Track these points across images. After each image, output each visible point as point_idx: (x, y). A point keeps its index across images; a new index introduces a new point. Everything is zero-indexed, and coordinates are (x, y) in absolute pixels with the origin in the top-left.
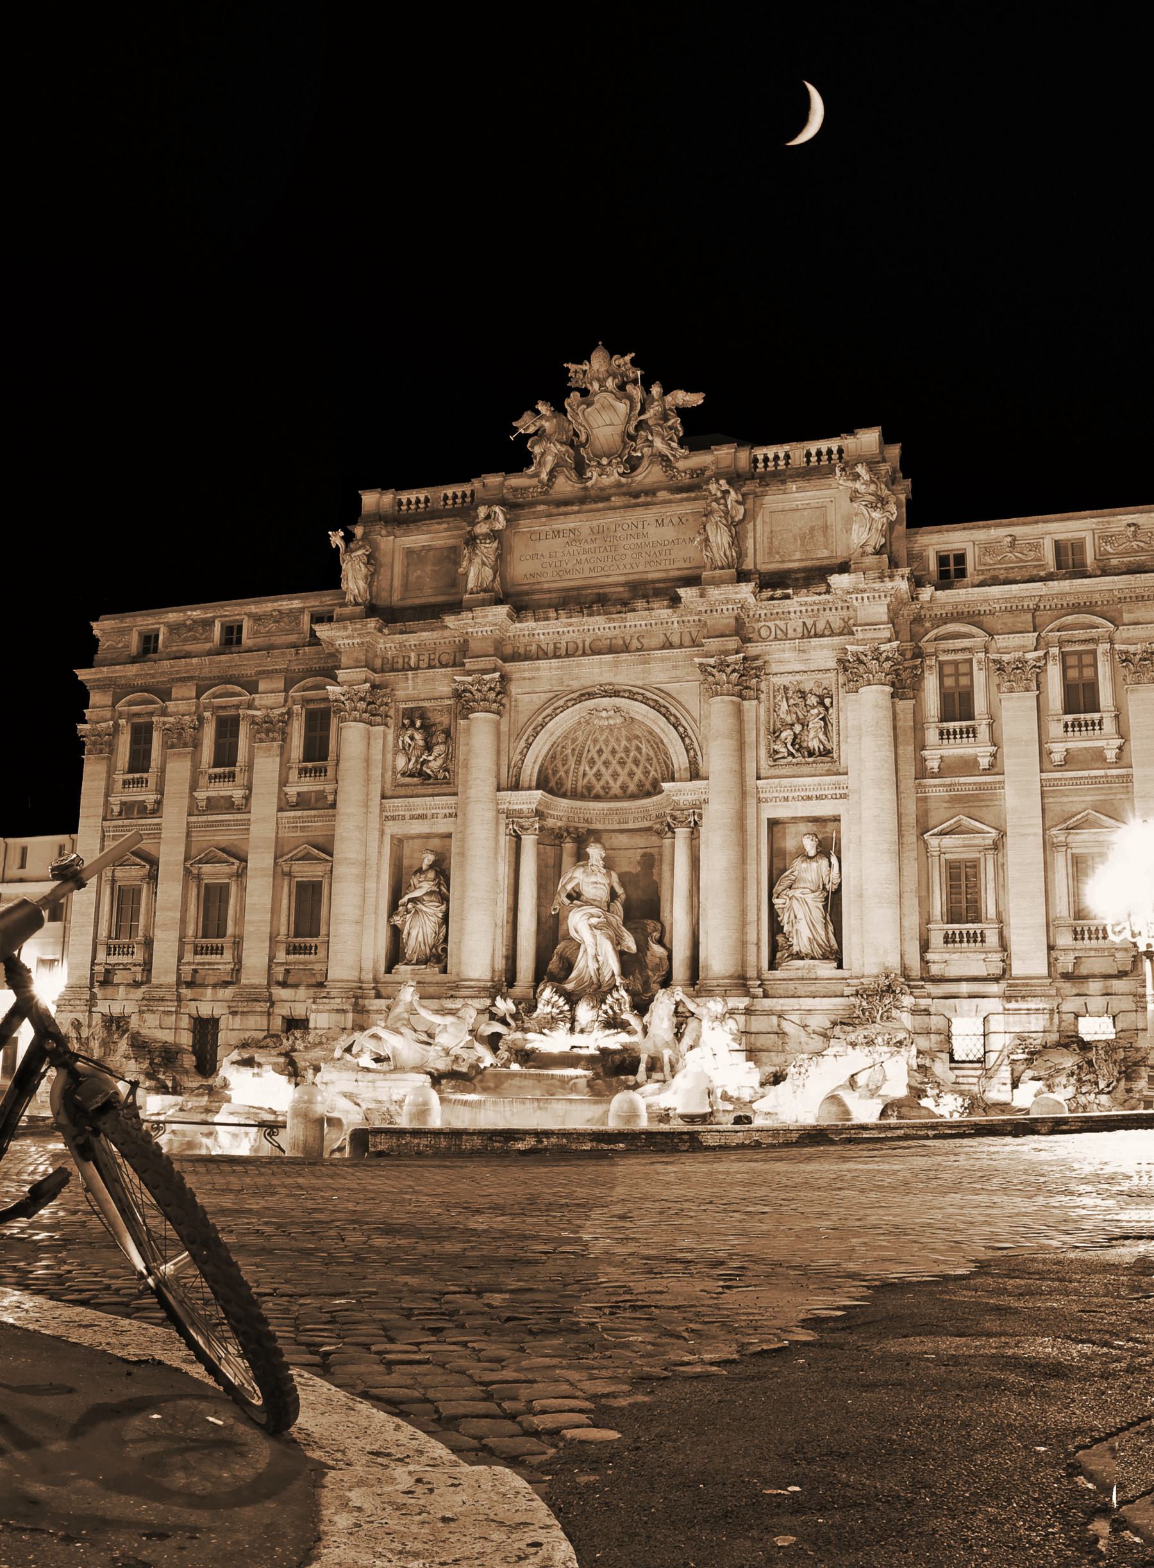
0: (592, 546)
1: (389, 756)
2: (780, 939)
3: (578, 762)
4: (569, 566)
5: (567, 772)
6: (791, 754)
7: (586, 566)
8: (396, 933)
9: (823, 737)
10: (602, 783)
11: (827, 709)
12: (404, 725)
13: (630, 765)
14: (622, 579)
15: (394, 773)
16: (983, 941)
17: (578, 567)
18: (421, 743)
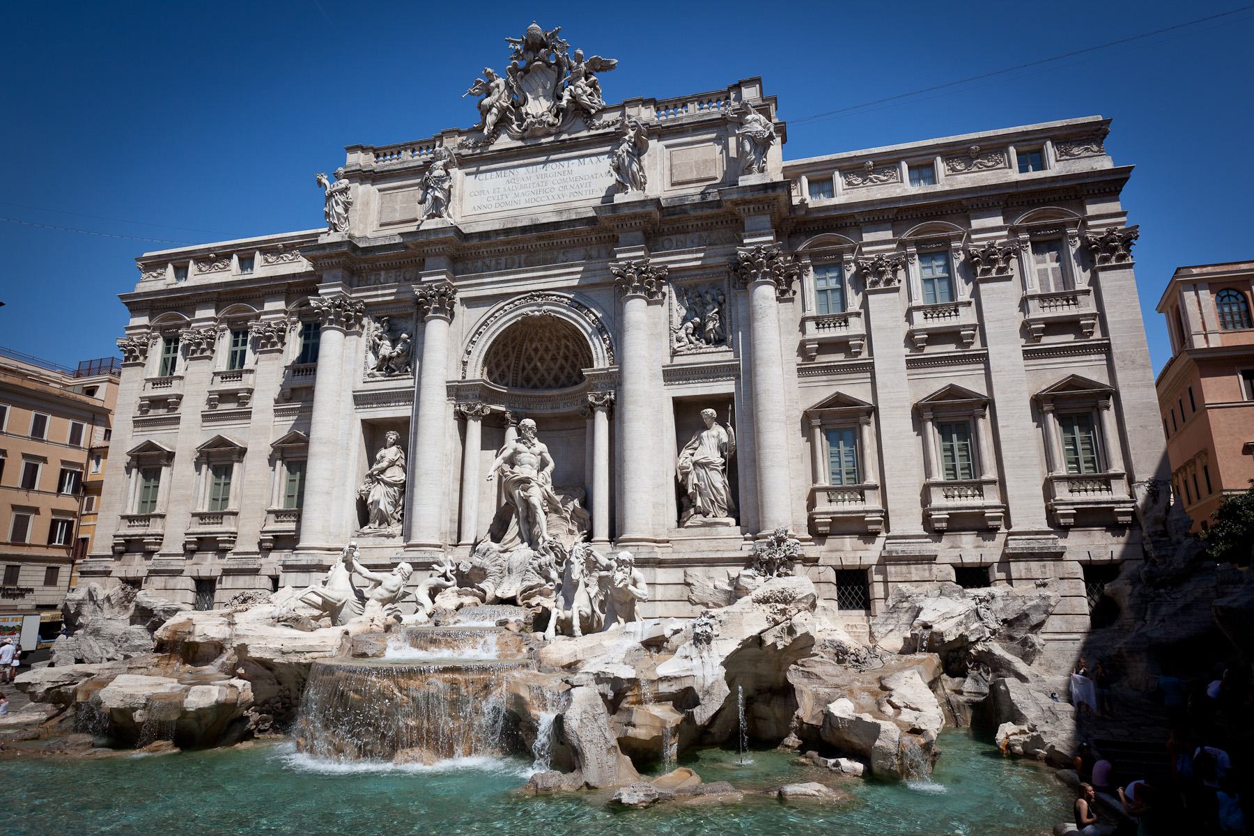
1: (361, 355)
2: (684, 500)
3: (518, 358)
5: (509, 367)
6: (691, 342)
7: (522, 199)
10: (539, 375)
11: (720, 305)
13: (561, 361)
14: (551, 208)
16: (863, 500)
18: (388, 343)
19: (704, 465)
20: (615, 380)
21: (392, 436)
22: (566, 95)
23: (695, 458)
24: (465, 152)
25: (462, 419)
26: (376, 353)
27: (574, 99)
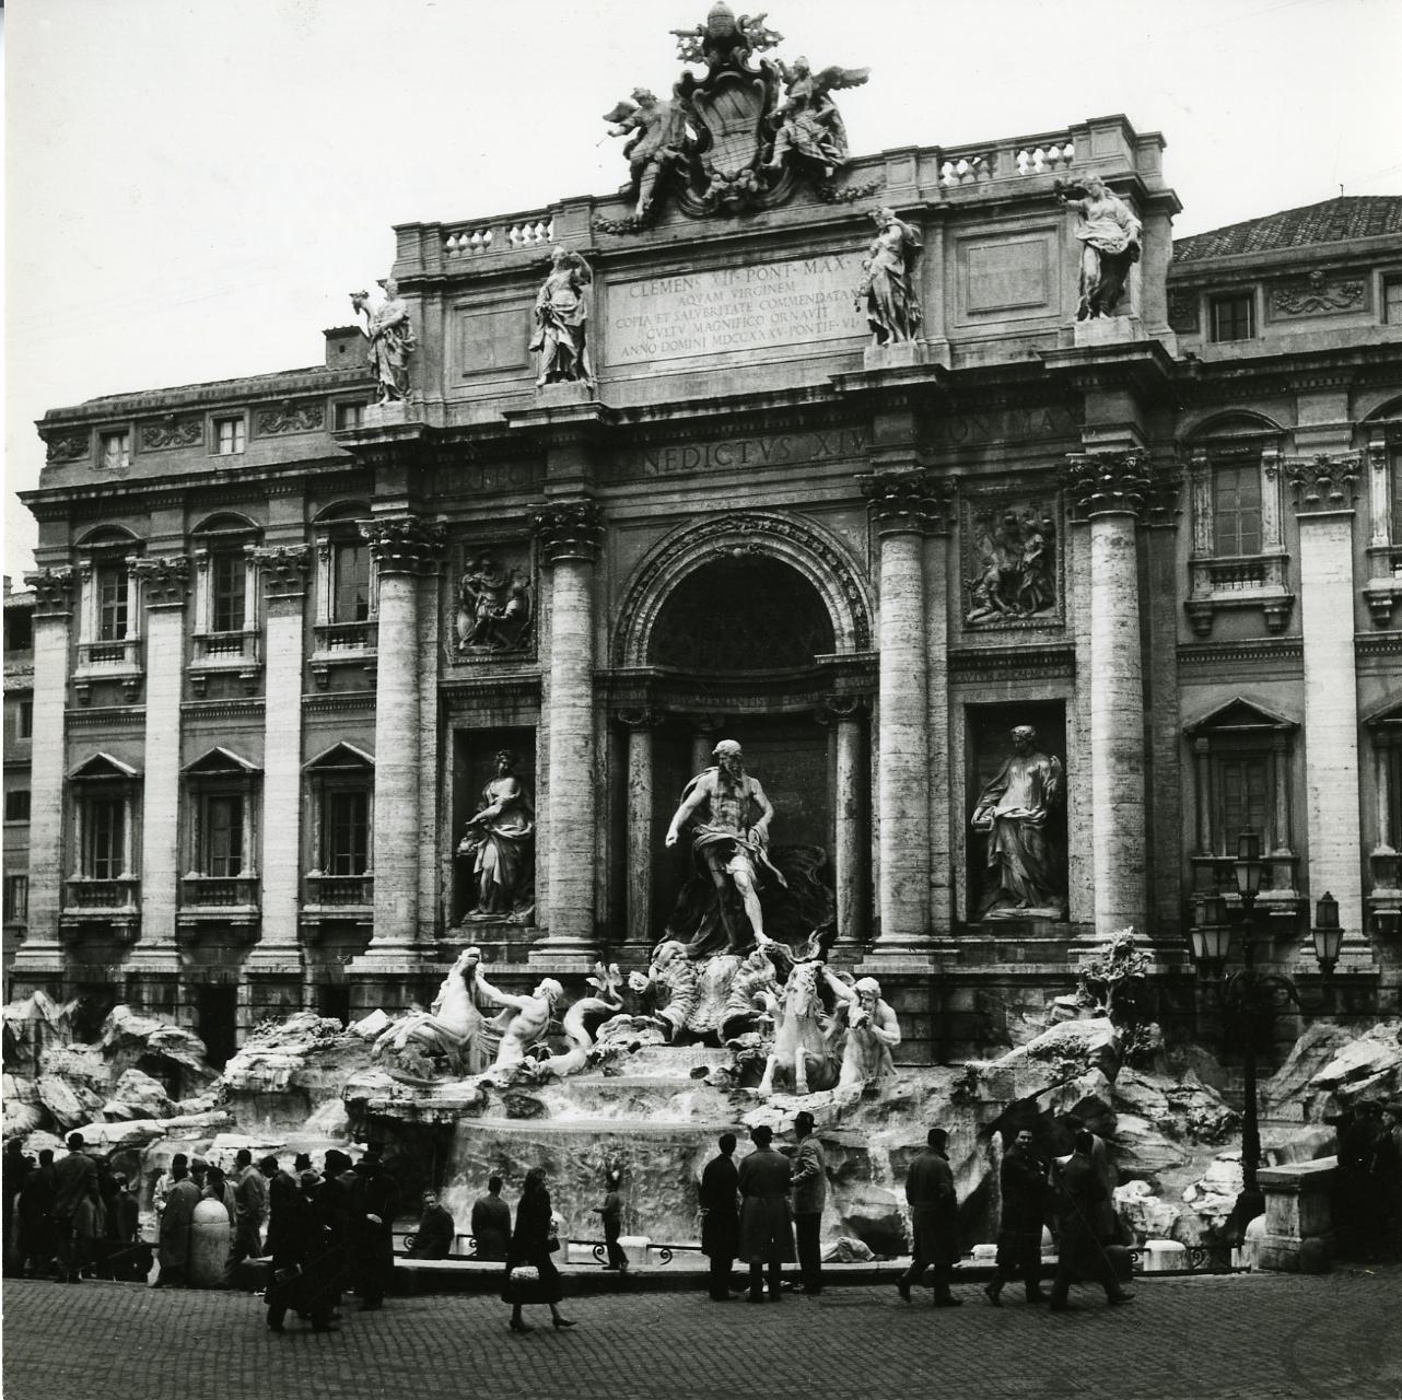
0: (716, 304)
4: (686, 335)
15: (457, 640)
17: (698, 336)
19: (1015, 823)
20: (866, 669)
22: (780, 148)
23: (998, 811)
24: (608, 242)
26: (472, 613)
27: (794, 155)
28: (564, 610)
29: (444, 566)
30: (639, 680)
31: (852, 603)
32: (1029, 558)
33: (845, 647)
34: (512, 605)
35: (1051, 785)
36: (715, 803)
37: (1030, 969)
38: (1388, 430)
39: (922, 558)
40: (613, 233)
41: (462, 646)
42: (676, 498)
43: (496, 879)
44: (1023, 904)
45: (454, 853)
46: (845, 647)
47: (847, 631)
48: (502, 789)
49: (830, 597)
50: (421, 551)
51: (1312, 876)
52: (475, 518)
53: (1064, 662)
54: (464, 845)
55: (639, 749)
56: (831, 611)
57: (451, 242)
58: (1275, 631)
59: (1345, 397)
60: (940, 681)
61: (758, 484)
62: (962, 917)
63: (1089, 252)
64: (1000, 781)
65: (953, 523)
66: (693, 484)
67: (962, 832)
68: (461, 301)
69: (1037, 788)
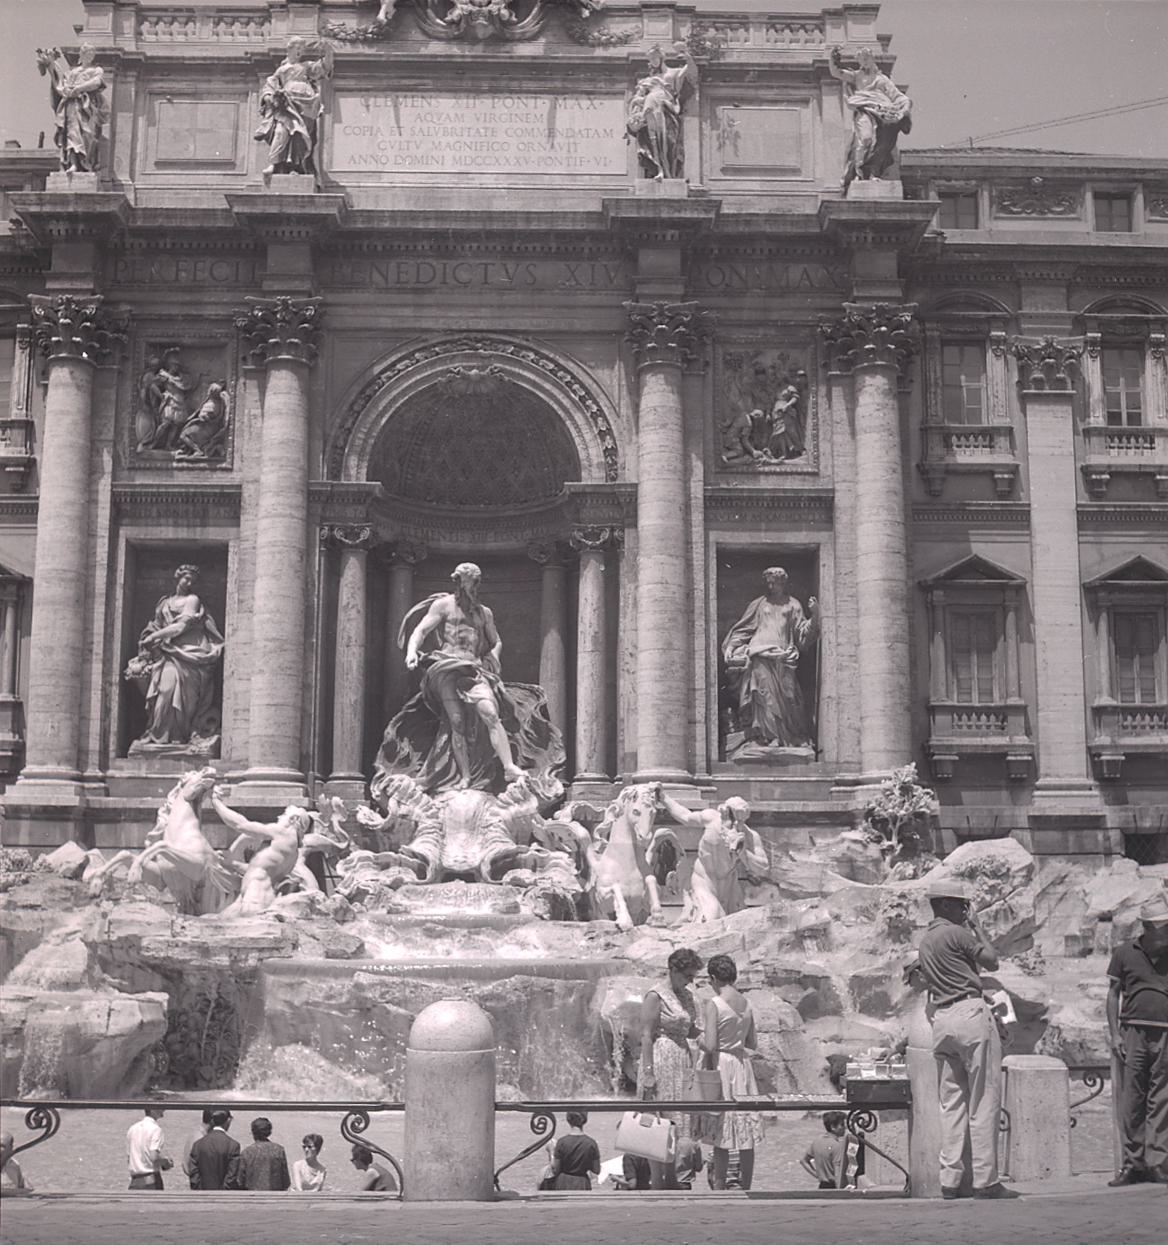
8: (133, 694)
9: (793, 430)
11: (800, 391)
12: (148, 366)
14: (504, 182)
15: (134, 442)
19: (770, 662)
20: (622, 503)
21: (184, 573)
25: (334, 555)
28: (271, 424)
29: (124, 359)
30: (361, 496)
31: (602, 434)
32: (782, 405)
33: (592, 476)
34: (208, 406)
35: (804, 625)
36: (451, 629)
37: (787, 806)
38: (1101, 325)
39: (683, 393)
40: (343, 40)
41: (140, 448)
42: (407, 312)
43: (176, 704)
44: (775, 743)
45: (122, 675)
46: (592, 476)
47: (595, 462)
48: (185, 606)
49: (577, 427)
50: (102, 340)
51: (1042, 724)
52: (165, 310)
53: (821, 507)
54: (135, 665)
55: (353, 574)
56: (577, 440)
57: (146, 26)
58: (1002, 496)
59: (1064, 290)
60: (697, 517)
61: (501, 306)
62: (715, 756)
63: (864, 118)
64: (748, 621)
65: (707, 364)
66: (428, 299)
67: (714, 669)
68: (156, 86)
69: (790, 630)
